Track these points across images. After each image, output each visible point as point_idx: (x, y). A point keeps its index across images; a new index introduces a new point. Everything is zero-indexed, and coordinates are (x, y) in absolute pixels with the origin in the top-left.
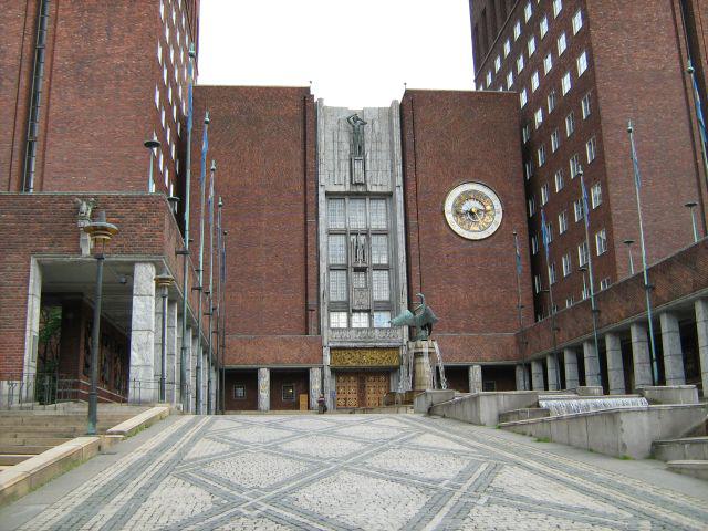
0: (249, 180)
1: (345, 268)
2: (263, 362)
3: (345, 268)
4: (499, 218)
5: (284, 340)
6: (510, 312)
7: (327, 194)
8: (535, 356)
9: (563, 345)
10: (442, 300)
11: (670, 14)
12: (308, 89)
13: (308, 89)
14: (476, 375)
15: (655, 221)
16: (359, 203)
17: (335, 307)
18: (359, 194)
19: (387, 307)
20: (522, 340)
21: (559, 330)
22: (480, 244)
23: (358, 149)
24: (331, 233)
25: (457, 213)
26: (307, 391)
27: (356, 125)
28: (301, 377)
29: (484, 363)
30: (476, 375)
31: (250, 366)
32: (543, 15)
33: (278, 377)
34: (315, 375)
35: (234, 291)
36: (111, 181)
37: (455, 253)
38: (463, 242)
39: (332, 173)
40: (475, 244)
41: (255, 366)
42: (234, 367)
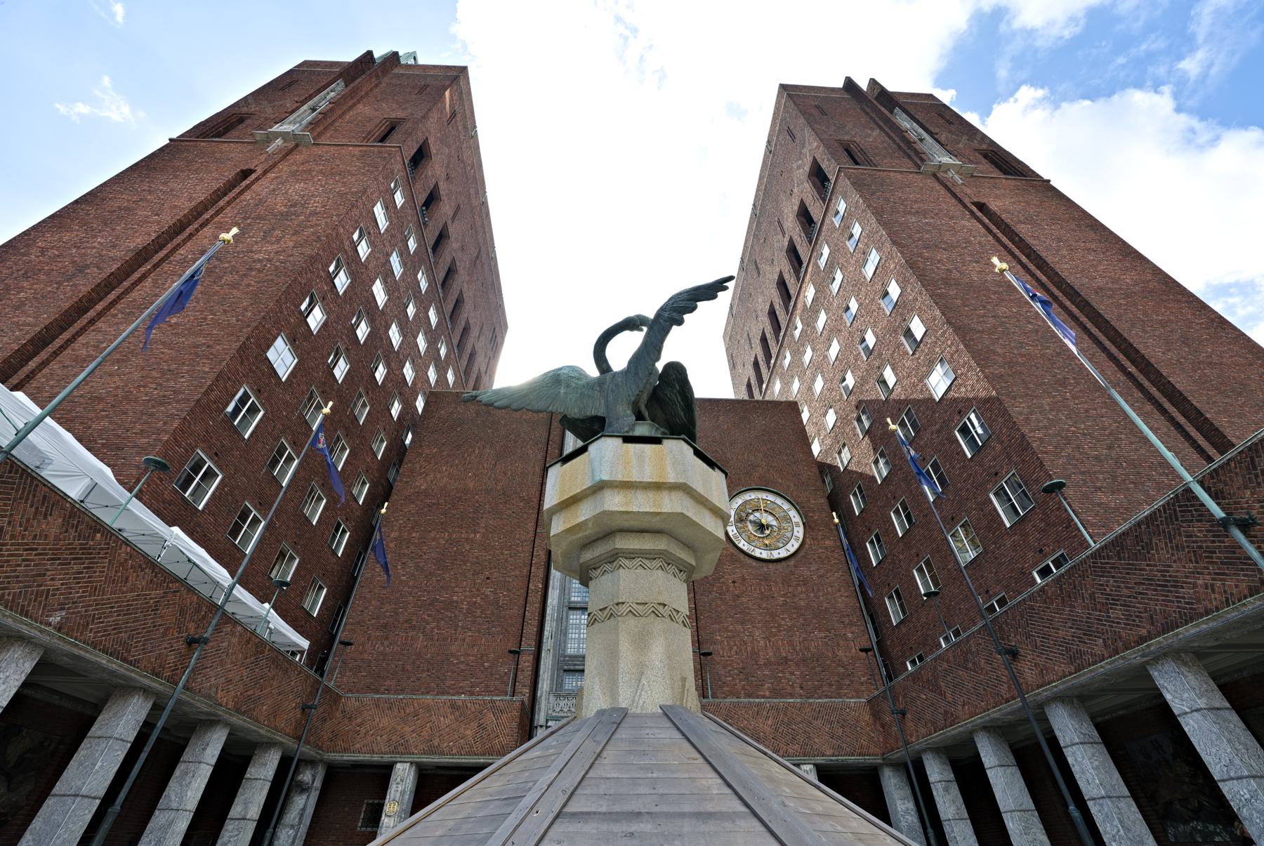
0: (471, 485)
2: (402, 749)
4: (799, 532)
5: (454, 706)
6: (842, 670)
8: (937, 737)
9: (1044, 693)
10: (731, 649)
11: (990, 238)
15: (1110, 448)
20: (889, 709)
21: (1014, 654)
22: (779, 566)
29: (820, 760)
31: (376, 758)
32: (818, 312)
35: (413, 628)
36: (154, 374)
37: (744, 580)
38: (754, 563)
40: (771, 565)
41: (387, 758)
42: (347, 757)
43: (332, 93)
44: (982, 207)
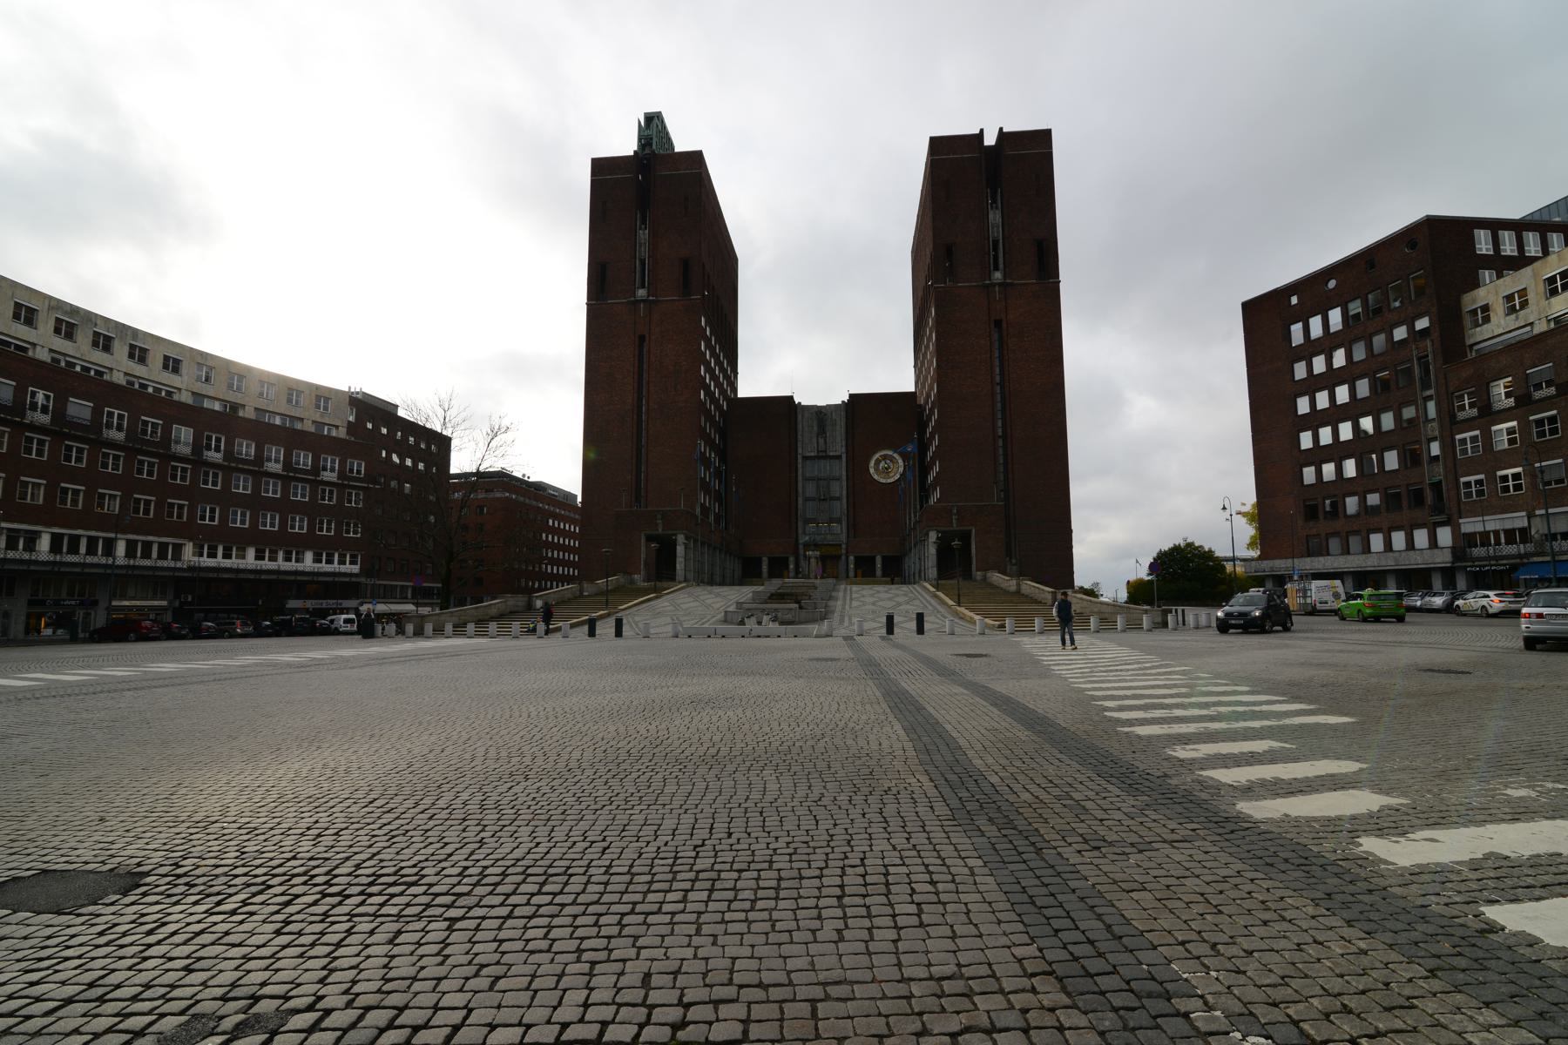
1: (813, 499)
3: (813, 499)
7: (805, 458)
12: (791, 398)
13: (791, 398)
14: (879, 560)
16: (822, 462)
17: (807, 521)
18: (823, 456)
19: (839, 521)
23: (822, 431)
24: (806, 479)
25: (876, 469)
26: (787, 567)
27: (820, 414)
28: (785, 562)
30: (879, 560)
33: (772, 561)
34: (792, 559)
39: (808, 444)
43: (643, 235)
44: (998, 323)
